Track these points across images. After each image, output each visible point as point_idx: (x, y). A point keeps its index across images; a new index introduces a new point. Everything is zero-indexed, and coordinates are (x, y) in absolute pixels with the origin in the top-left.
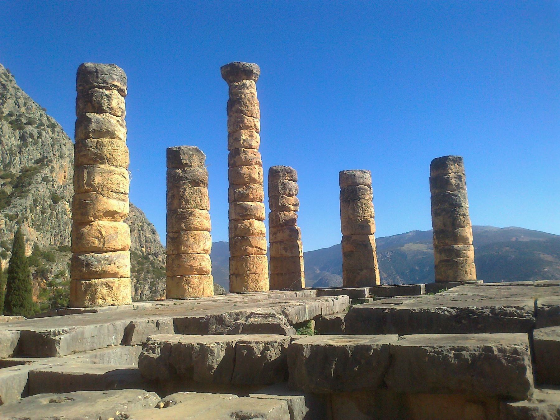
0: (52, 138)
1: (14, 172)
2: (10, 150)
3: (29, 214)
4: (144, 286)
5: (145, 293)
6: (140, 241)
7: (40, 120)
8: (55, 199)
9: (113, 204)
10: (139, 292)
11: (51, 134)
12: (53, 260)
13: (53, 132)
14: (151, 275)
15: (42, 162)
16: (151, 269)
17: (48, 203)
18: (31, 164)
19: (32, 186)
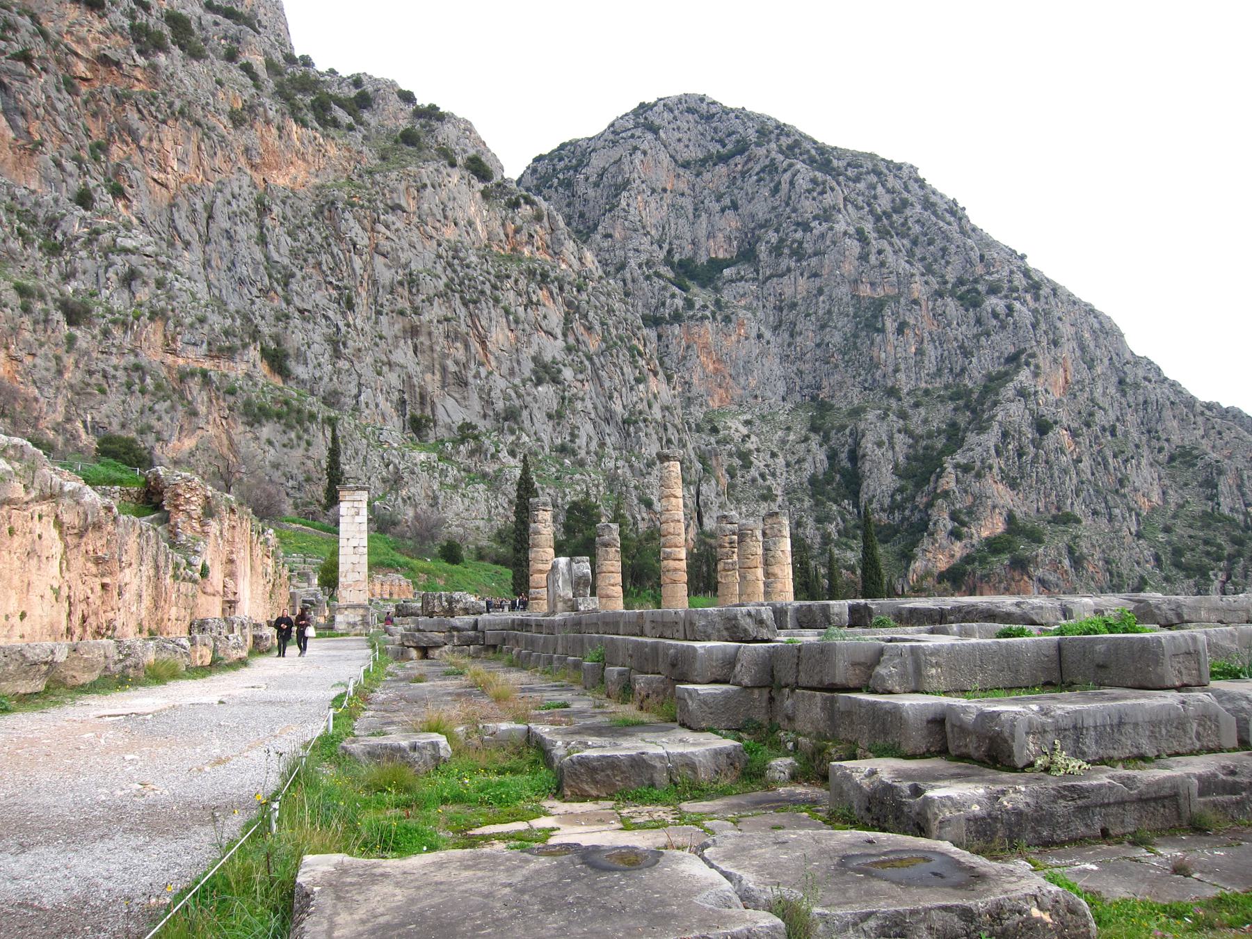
0: (1035, 312)
1: (970, 385)
2: (960, 347)
3: (995, 462)
6: (1243, 495)
7: (1010, 281)
8: (1043, 427)
12: (1040, 541)
13: (1037, 298)
18: (996, 369)
19: (999, 408)
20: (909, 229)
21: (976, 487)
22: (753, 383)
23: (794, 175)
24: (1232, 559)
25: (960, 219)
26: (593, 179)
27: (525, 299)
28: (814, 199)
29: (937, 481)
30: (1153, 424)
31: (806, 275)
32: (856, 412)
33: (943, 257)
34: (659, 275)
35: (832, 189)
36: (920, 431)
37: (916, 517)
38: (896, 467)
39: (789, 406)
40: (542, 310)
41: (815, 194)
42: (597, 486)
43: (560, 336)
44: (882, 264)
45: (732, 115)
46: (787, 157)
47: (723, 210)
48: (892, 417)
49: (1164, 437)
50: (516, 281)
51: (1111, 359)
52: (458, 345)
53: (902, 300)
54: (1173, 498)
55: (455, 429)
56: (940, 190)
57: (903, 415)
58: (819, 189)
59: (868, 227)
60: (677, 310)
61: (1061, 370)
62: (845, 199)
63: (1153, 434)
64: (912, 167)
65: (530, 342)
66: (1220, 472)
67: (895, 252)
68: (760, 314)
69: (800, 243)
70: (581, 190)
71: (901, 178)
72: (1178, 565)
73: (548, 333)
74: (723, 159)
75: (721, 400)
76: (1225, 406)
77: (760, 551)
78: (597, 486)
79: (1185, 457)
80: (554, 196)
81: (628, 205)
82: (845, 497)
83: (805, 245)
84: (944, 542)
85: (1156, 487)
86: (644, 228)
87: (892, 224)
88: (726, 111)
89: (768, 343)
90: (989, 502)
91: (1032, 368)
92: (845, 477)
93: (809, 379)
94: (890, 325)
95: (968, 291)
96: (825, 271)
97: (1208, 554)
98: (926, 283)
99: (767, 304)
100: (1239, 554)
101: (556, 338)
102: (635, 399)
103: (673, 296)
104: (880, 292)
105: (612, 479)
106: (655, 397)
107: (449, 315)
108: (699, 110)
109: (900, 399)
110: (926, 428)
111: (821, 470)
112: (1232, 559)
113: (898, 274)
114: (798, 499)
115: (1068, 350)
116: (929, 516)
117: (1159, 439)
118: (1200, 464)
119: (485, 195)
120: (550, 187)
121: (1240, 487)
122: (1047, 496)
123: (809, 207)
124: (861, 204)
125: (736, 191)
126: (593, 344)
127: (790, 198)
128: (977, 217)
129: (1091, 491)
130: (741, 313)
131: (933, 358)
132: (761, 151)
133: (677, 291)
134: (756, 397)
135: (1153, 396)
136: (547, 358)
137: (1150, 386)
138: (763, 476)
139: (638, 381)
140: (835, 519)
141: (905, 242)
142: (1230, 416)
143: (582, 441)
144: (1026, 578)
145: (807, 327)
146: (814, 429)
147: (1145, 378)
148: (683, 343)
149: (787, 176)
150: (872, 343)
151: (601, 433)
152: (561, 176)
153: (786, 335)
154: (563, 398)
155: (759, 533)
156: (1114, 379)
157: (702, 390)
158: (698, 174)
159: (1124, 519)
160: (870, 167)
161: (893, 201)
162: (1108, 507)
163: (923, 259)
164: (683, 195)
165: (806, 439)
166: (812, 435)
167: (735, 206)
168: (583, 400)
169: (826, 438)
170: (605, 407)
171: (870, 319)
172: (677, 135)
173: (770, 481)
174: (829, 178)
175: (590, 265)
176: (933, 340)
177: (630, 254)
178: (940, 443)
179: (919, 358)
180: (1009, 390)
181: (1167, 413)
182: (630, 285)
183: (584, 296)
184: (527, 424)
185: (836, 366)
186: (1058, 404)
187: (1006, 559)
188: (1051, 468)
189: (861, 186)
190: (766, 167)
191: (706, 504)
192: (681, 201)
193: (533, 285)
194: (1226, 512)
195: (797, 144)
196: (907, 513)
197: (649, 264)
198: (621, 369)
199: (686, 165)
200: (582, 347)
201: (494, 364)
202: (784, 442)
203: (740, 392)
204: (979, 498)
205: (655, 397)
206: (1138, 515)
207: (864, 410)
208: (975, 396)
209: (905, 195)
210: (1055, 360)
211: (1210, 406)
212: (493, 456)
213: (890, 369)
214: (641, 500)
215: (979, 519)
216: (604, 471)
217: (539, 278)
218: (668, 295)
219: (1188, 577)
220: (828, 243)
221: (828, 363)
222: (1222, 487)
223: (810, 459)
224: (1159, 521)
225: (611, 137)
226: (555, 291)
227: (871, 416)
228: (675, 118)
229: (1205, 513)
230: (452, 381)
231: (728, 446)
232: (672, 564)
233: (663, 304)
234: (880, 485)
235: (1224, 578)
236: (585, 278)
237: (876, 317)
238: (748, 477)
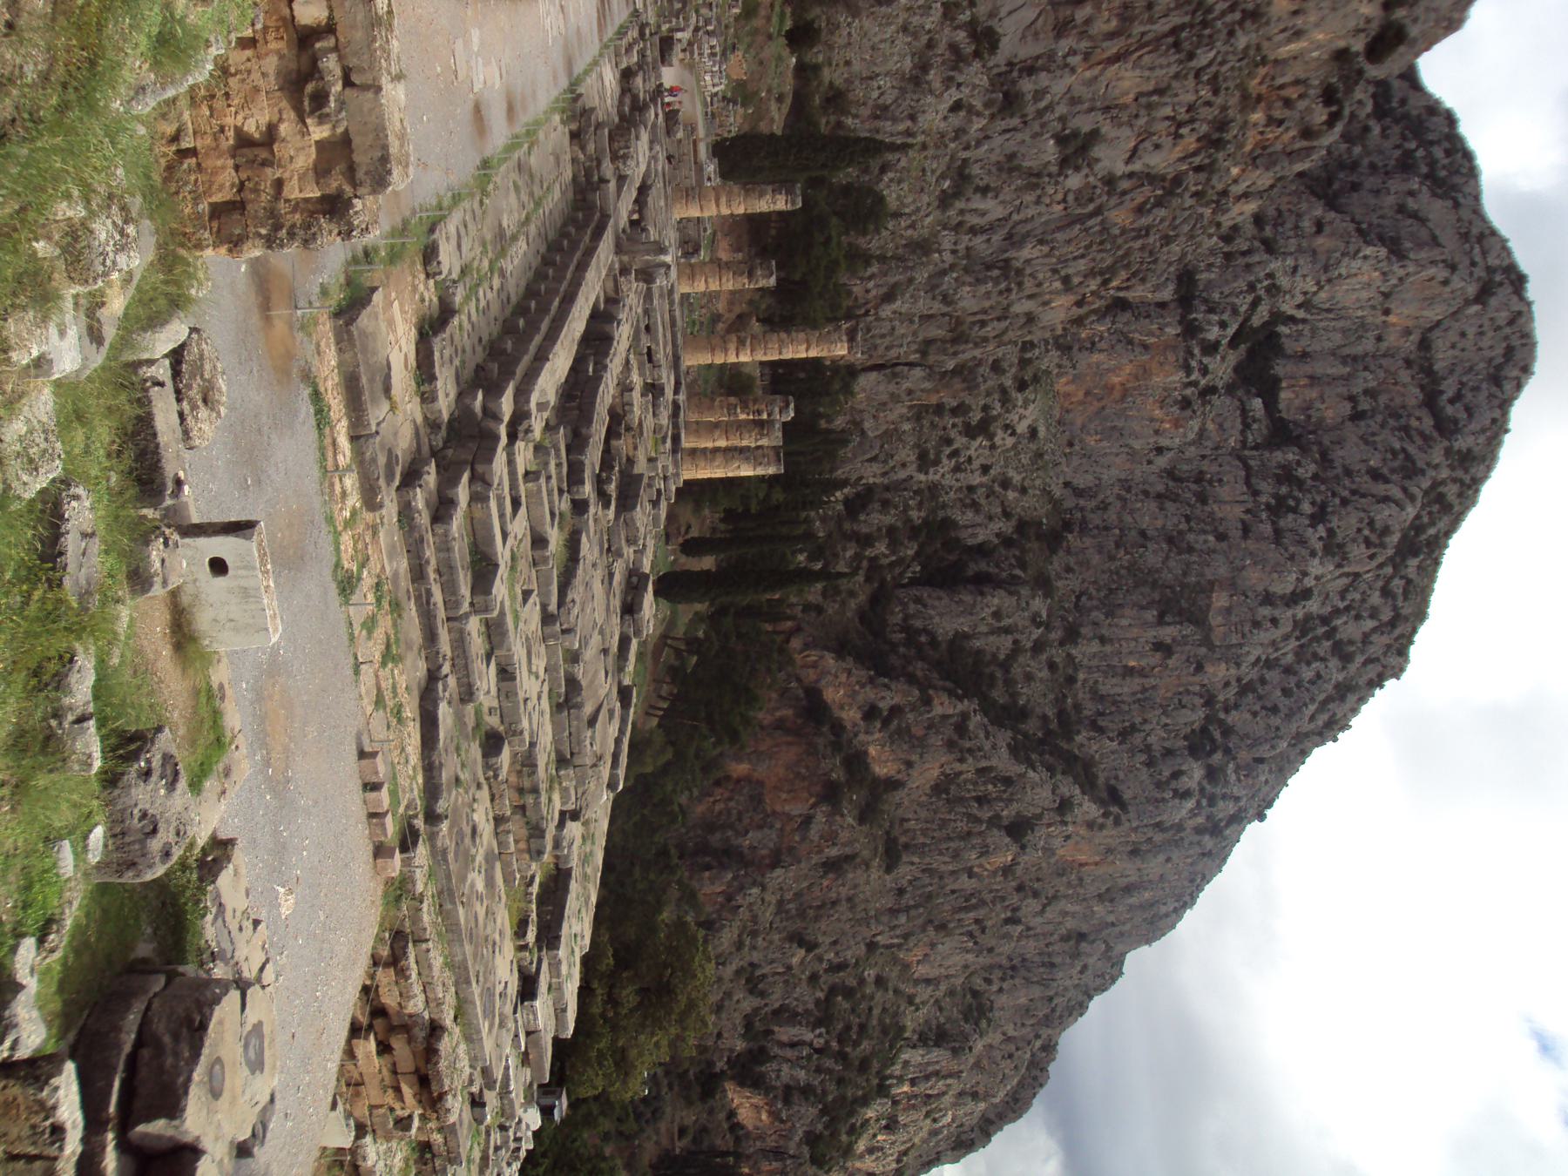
0: (1179, 827)
1: (1079, 739)
3: (969, 767)
4: (802, 1068)
5: (785, 1068)
6: (927, 1078)
8: (1018, 830)
9: (723, 200)
10: (789, 1053)
11: (1191, 823)
12: (862, 819)
13: (1199, 831)
14: (831, 1087)
15: (1113, 797)
17: (1005, 813)
19: (1045, 774)
20: (1308, 664)
21: (936, 740)
22: (1091, 441)
23: (1397, 503)
24: (842, 1056)
25: (1320, 734)
26: (1411, 204)
27: (1183, 115)
28: (1359, 530)
29: (944, 689)
30: (1023, 972)
31: (1247, 517)
32: (1043, 584)
33: (1263, 708)
34: (1255, 304)
35: (1372, 557)
36: (1017, 671)
37: (894, 660)
38: (966, 636)
39: (1058, 492)
40: (1167, 141)
41: (1366, 532)
42: (912, 226)
43: (1130, 168)
44: (1256, 624)
45: (1497, 414)
46: (1426, 493)
47: (1352, 398)
48: (1037, 633)
49: (1005, 986)
50: (1208, 104)
51: (1113, 924)
52: (1114, 23)
53: (1203, 650)
54: (923, 993)
55: (989, 23)
56: (1364, 708)
57: (1038, 647)
58: (1374, 538)
59: (1313, 606)
60: (1201, 330)
61: (1097, 858)
62: (1357, 575)
63: (1010, 973)
64: (1402, 670)
65: (1120, 125)
66: (955, 1052)
67: (1273, 643)
68: (1192, 451)
69: (1295, 510)
70: (1395, 185)
71: (1385, 654)
72: (833, 991)
73: (1133, 154)
74: (1430, 401)
75: (1067, 395)
76: (1052, 1068)
77: (745, 443)
78: (912, 226)
79: (977, 1009)
80: (1388, 144)
81: (1365, 257)
82: (923, 568)
83: (1291, 516)
84: (860, 698)
86: (1329, 281)
87: (1317, 639)
88: (1505, 405)
89: (1150, 462)
90: (915, 758)
91: (1100, 820)
92: (951, 565)
93: (1095, 519)
94: (1168, 633)
95: (1213, 741)
96: (1251, 544)
97: (848, 1028)
98: (1227, 684)
99: (1206, 462)
101: (1127, 163)
102: (1041, 276)
103: (1223, 325)
104: (1215, 620)
105: (923, 247)
106: (1045, 304)
107: (1157, 8)
108: (1510, 363)
109: (1062, 644)
110: (1020, 678)
111: (963, 534)
112: (842, 1056)
113: (1241, 645)
114: (920, 504)
115: (1126, 869)
116: (897, 678)
118: (968, 1027)
119: (1342, 55)
120: (1404, 138)
121: (937, 1073)
122: (924, 832)
123: (1347, 523)
124: (1349, 597)
125: (1379, 418)
126: (1120, 216)
127: (1363, 496)
128: (1322, 758)
130: (1195, 424)
131: (1118, 690)
132: (1437, 455)
133: (1231, 331)
134: (1071, 444)
135: (1061, 974)
136: (1098, 151)
137: (1075, 972)
138: (955, 453)
139: (1066, 280)
140: (893, 553)
141: (1290, 658)
142: (1038, 1073)
143: (978, 203)
144: (812, 800)
145: (1171, 517)
146: (1022, 526)
147: (1085, 967)
148: (1153, 340)
149: (1396, 492)
150: (1142, 608)
151: (990, 228)
152: (1420, 153)
153: (1160, 488)
154: (1038, 175)
155: (764, 442)
156: (1084, 928)
157: (1082, 366)
158: (1408, 363)
159: (893, 928)
160: (1404, 612)
161: (1351, 642)
162: (908, 909)
163: (1263, 681)
164: (1379, 339)
165: (1007, 515)
166: (1013, 522)
167: (1357, 416)
168: (1038, 202)
169: (1007, 542)
170: (1028, 234)
171: (1180, 604)
172: (1471, 332)
173: (947, 464)
174: (1390, 552)
175: (1236, 210)
176: (1144, 690)
177: (1290, 262)
178: (999, 695)
179: (1120, 671)
180: (1069, 788)
181: (1037, 992)
182: (1241, 261)
183: (1189, 202)
184: (1001, 124)
185: (1112, 558)
186: (1049, 851)
187: (838, 775)
188: (962, 838)
189: (1376, 599)
190: (1413, 462)
191: (895, 375)
192: (1371, 335)
193: (1204, 128)
194: (904, 1056)
195: (1446, 508)
196: (902, 650)
197: (1273, 290)
198: (1083, 256)
199: (1425, 344)
200: (1114, 201)
201: (1088, 74)
202: (1006, 484)
203: (1079, 422)
204: (920, 744)
205: (1045, 304)
206: (899, 946)
207: (1048, 594)
208: (1065, 746)
209: (1360, 659)
210: (1110, 851)
211: (1049, 1048)
212: (951, 79)
213: (1104, 632)
214: (895, 286)
215: (892, 743)
216: (936, 236)
217: (1216, 136)
218: (1225, 317)
219: (818, 1002)
220: (1292, 549)
221: (1118, 546)
223: (979, 519)
224: (893, 974)
225: (1475, 231)
226: (1197, 160)
227: (1039, 605)
228: (1499, 328)
229: (903, 1029)
230: (1061, 16)
231: (998, 405)
232: (732, 347)
233: (1211, 310)
234: (941, 615)
235: (816, 1045)
236: (1217, 202)
237: (1180, 614)
238: (953, 434)
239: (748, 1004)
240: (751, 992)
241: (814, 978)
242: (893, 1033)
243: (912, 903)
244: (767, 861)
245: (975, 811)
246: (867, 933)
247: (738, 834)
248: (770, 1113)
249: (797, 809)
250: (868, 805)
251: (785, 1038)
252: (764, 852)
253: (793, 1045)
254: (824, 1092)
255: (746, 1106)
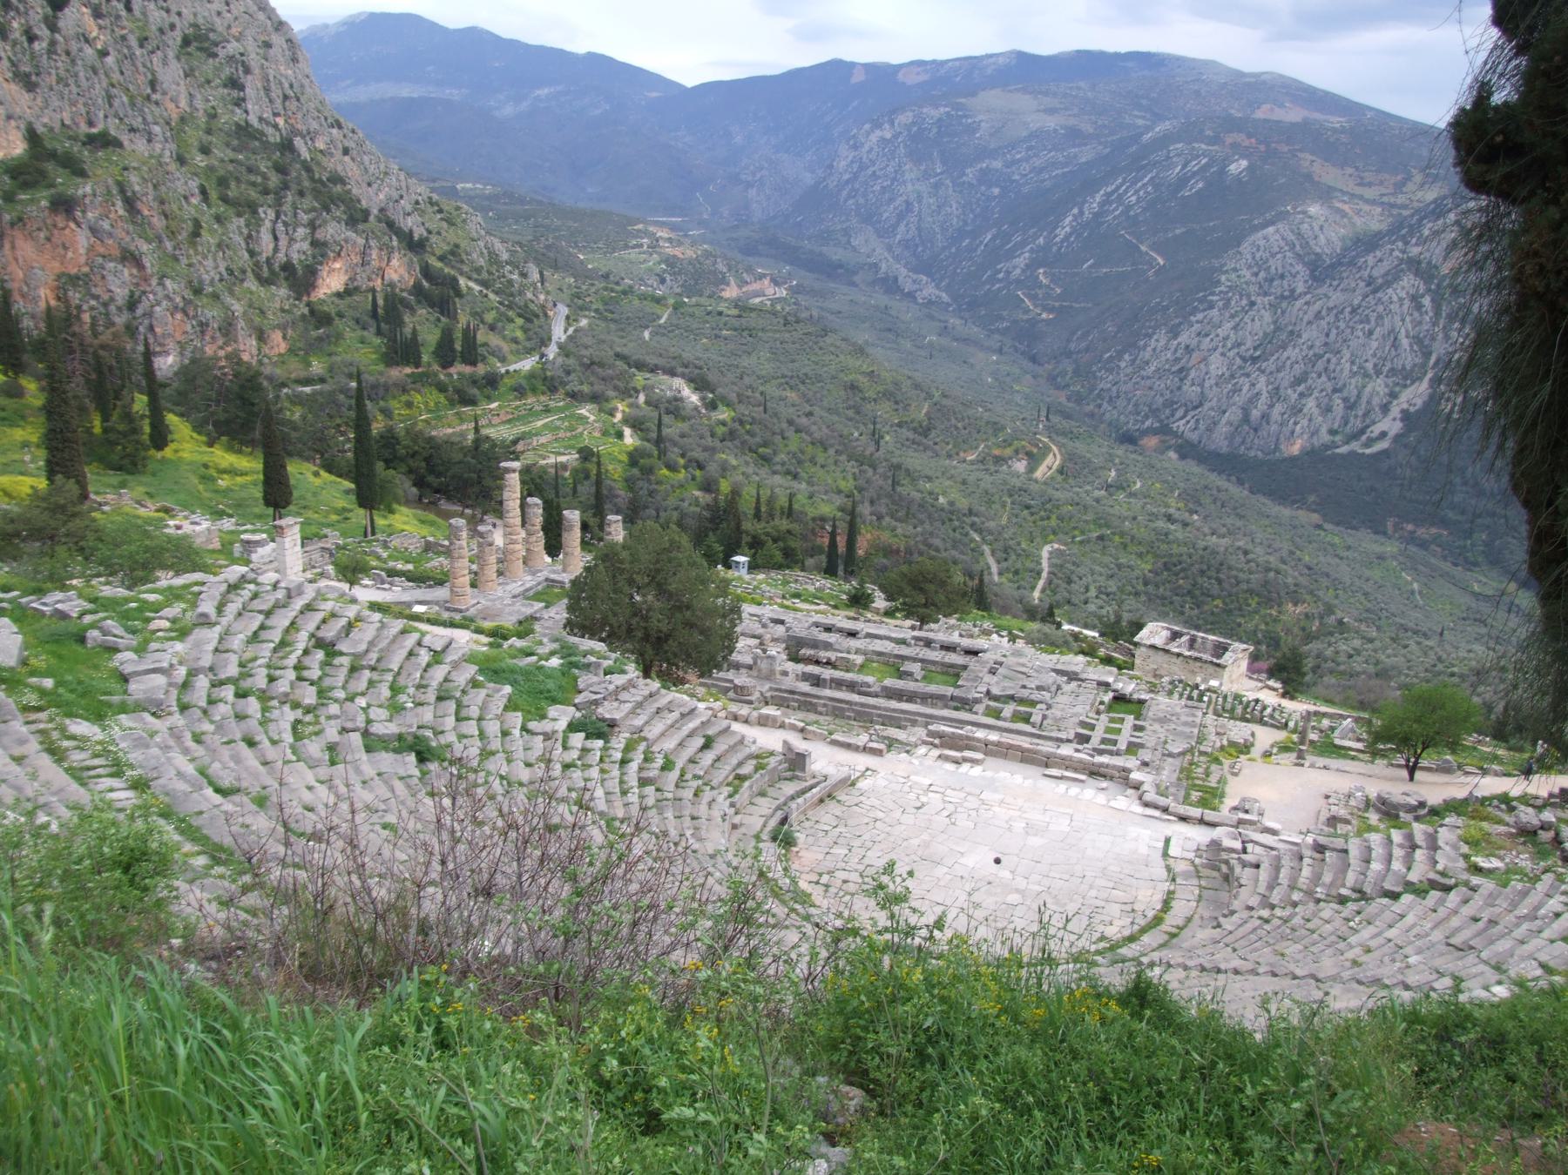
5: (296, 246)
10: (283, 243)
12: (82, 174)
16: (306, 184)
49: (174, 9)
72: (225, 199)
85: (182, 88)
100: (286, 186)
117: (168, 11)
118: (222, 53)
121: (267, 90)
122: (73, 104)
129: (125, 99)
144: (73, 225)
188: (73, 61)
219: (239, 215)
222: (249, 92)
224: (194, 136)
229: (237, 125)
239: (251, 284)
240: (242, 281)
241: (218, 219)
242: (244, 132)
243: (140, 119)
244: (135, 271)
245: (44, 45)
246: (173, 167)
247: (112, 299)
248: (335, 260)
249: (82, 239)
250: (65, 167)
251: (271, 246)
252: (126, 272)
253: (276, 238)
254: (313, 209)
255: (332, 281)
